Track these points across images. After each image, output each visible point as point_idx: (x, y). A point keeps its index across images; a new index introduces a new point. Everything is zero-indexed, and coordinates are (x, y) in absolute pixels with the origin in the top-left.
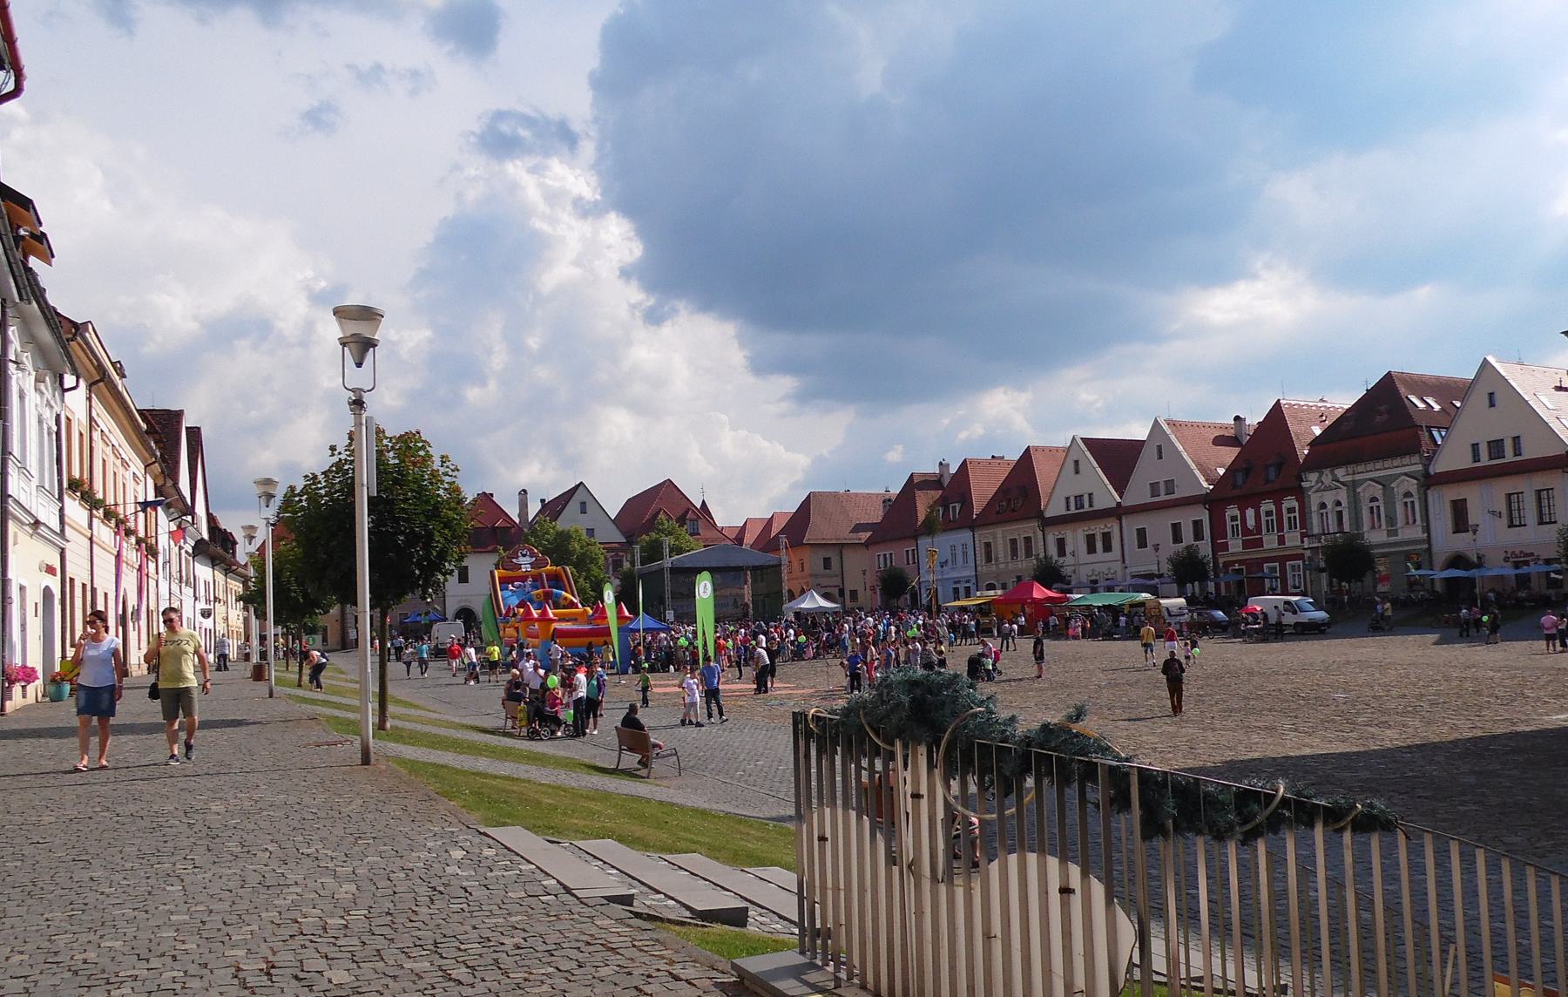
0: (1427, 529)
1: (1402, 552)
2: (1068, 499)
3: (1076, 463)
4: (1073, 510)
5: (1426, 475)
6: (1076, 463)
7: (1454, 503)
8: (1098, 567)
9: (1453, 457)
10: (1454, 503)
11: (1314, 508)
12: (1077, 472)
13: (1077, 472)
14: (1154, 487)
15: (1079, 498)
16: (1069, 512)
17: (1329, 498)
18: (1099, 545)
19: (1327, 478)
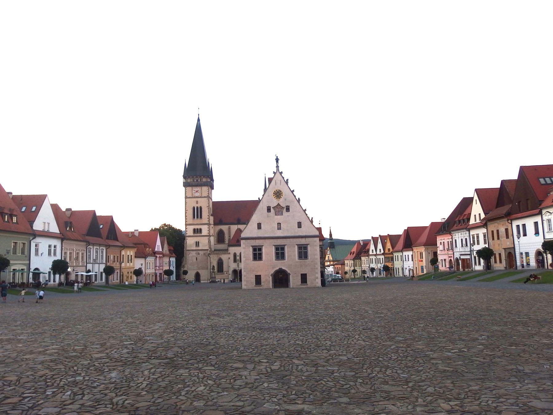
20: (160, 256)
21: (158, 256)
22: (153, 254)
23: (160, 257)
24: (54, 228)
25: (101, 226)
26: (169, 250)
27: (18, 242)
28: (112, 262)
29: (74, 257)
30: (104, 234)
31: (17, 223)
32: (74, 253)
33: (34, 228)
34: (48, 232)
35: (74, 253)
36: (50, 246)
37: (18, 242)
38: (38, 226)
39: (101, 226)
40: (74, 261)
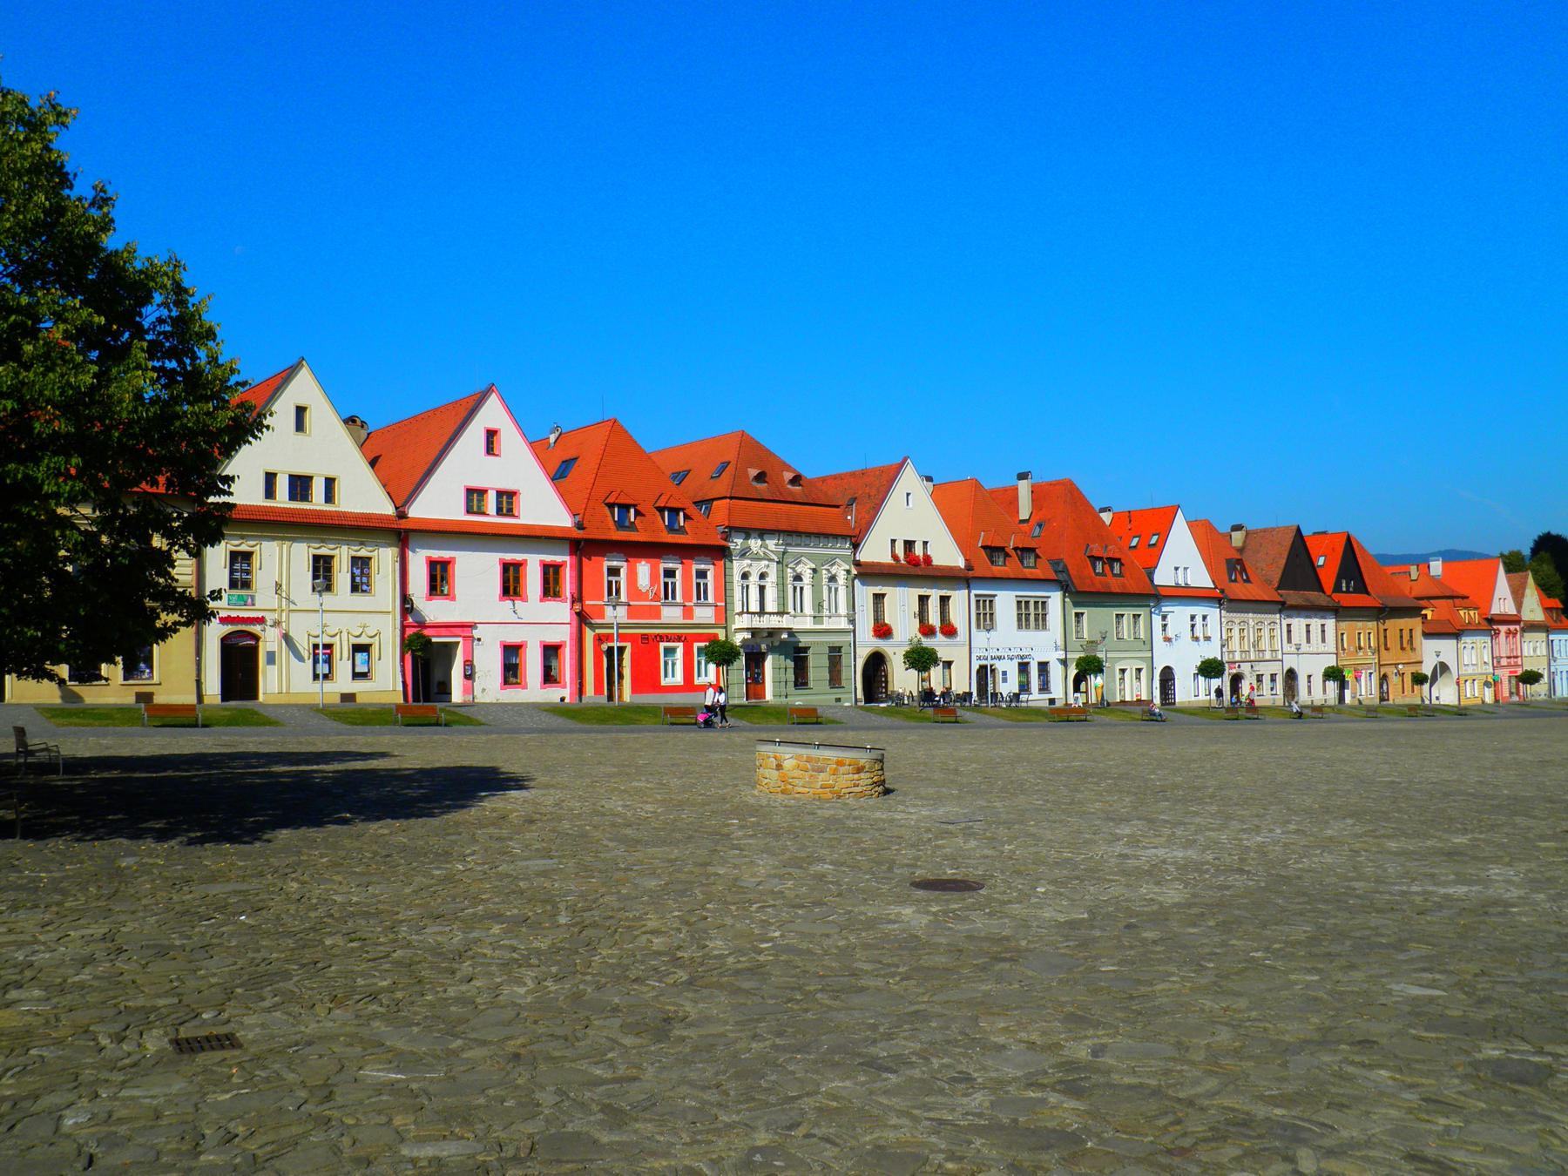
0: (852, 621)
1: (822, 643)
2: (270, 478)
3: (301, 411)
4: (282, 499)
5: (857, 564)
6: (301, 411)
7: (316, 558)
8: (336, 623)
9: (875, 550)
10: (316, 558)
11: (737, 577)
12: (300, 426)
13: (300, 426)
14: (474, 496)
15: (300, 486)
16: (269, 503)
17: (756, 569)
18: (342, 577)
19: (755, 544)
20: (1512, 628)
21: (1503, 628)
22: (1485, 623)
23: (1509, 633)
24: (1201, 578)
25: (1321, 561)
26: (1547, 610)
27: (1126, 613)
28: (1352, 648)
29: (1252, 640)
30: (1328, 580)
31: (1121, 575)
32: (1251, 630)
33: (1157, 582)
34: (1187, 587)
35: (1251, 630)
36: (1193, 618)
37: (1126, 613)
38: (1164, 576)
39: (1321, 561)
40: (1252, 650)
